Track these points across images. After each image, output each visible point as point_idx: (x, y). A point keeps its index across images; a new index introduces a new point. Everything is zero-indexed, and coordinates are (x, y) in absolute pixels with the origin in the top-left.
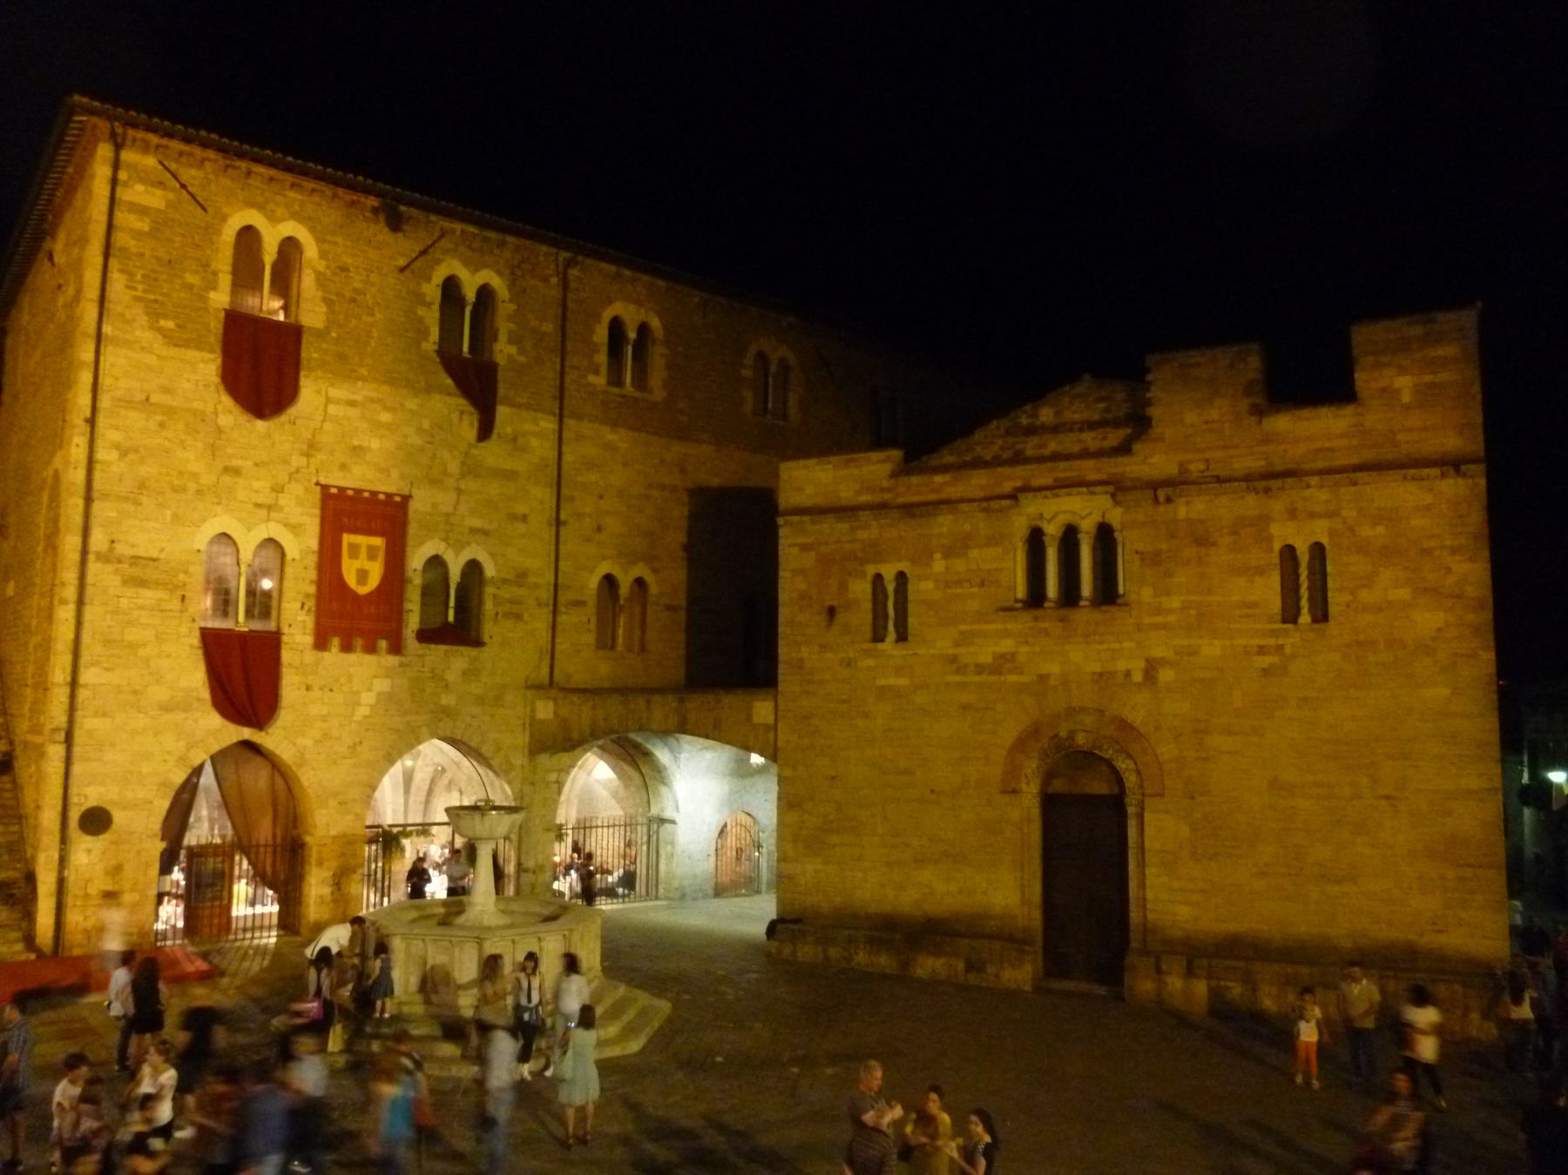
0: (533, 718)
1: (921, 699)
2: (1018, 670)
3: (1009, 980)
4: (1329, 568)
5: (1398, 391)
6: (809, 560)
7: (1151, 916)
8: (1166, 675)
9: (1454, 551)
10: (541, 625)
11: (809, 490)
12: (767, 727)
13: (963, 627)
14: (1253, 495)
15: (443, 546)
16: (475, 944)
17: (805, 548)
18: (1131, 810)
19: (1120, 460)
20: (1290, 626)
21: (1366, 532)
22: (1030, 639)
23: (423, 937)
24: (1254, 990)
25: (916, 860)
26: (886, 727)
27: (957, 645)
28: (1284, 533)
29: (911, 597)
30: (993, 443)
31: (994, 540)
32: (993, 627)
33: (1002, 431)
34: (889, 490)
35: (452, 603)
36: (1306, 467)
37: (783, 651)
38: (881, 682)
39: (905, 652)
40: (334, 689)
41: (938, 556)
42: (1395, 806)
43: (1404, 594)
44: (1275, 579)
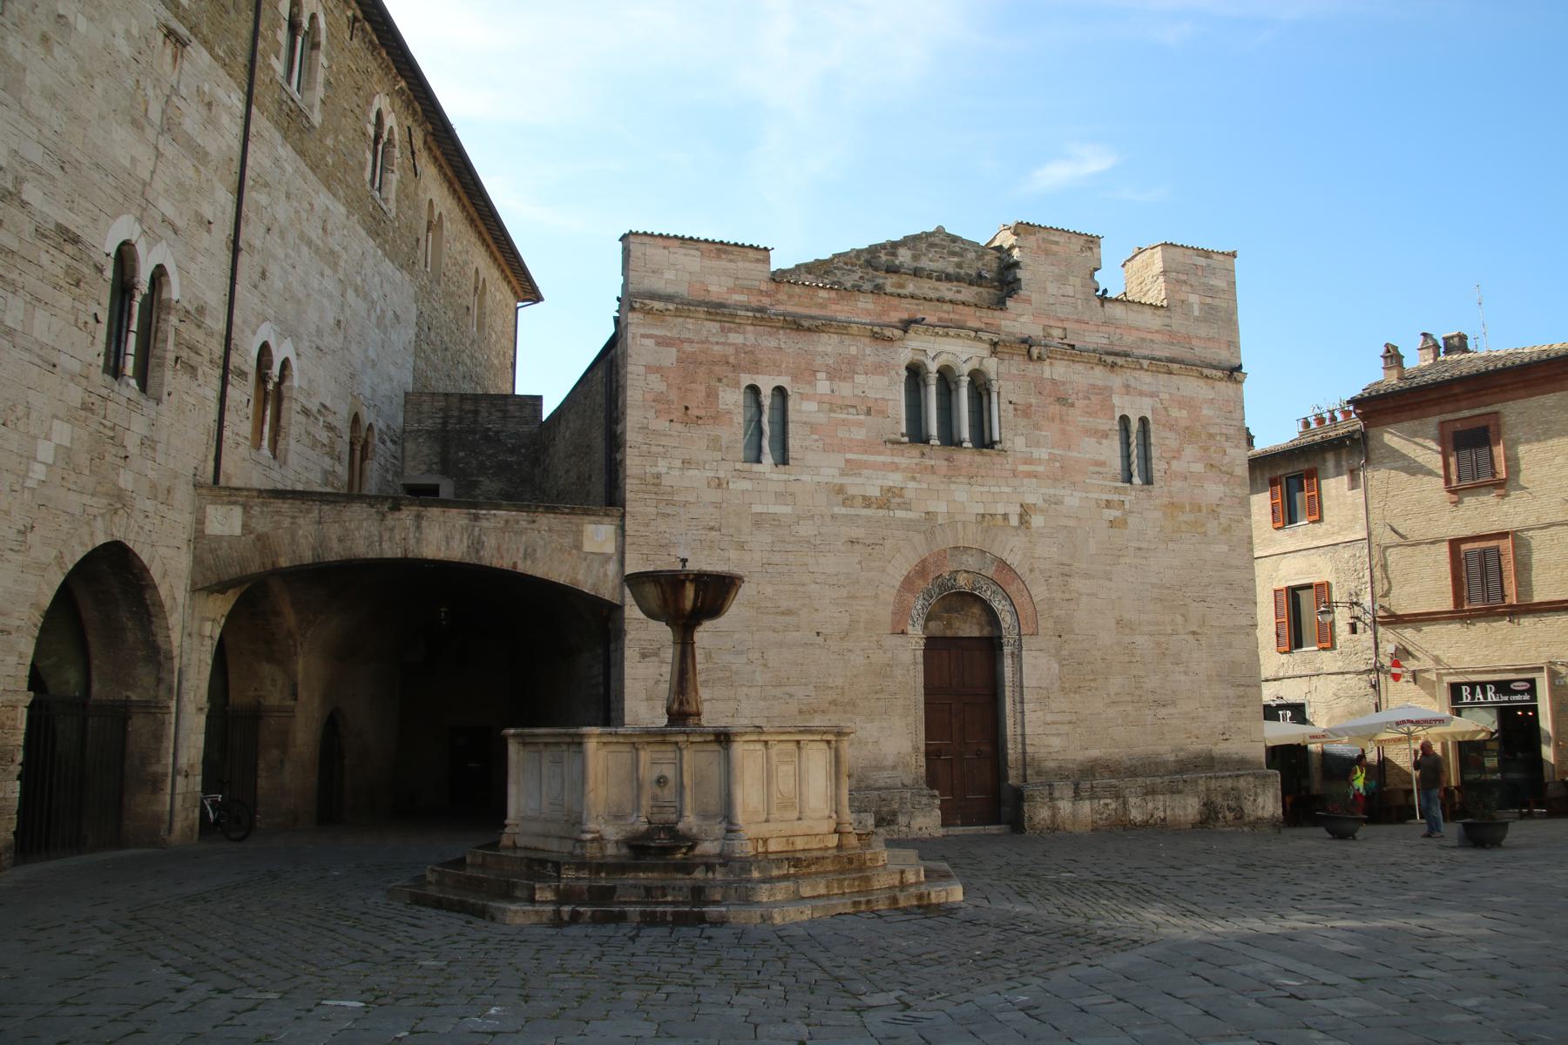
0: (198, 533)
1: (806, 530)
2: (906, 506)
3: (920, 829)
4: (1153, 440)
6: (669, 356)
7: (1029, 750)
8: (1037, 521)
9: (1228, 438)
11: (669, 275)
12: (606, 558)
13: (849, 456)
15: (137, 229)
16: (824, 746)
18: (1007, 650)
19: (997, 313)
20: (1128, 485)
22: (918, 476)
23: (798, 737)
24: (1125, 803)
25: (801, 712)
26: (765, 561)
27: (843, 474)
28: (1124, 405)
29: (792, 416)
30: (854, 272)
31: (879, 369)
35: (134, 327)
36: (1136, 352)
37: (634, 464)
38: (757, 508)
39: (786, 477)
40: (9, 423)
44: (1115, 444)
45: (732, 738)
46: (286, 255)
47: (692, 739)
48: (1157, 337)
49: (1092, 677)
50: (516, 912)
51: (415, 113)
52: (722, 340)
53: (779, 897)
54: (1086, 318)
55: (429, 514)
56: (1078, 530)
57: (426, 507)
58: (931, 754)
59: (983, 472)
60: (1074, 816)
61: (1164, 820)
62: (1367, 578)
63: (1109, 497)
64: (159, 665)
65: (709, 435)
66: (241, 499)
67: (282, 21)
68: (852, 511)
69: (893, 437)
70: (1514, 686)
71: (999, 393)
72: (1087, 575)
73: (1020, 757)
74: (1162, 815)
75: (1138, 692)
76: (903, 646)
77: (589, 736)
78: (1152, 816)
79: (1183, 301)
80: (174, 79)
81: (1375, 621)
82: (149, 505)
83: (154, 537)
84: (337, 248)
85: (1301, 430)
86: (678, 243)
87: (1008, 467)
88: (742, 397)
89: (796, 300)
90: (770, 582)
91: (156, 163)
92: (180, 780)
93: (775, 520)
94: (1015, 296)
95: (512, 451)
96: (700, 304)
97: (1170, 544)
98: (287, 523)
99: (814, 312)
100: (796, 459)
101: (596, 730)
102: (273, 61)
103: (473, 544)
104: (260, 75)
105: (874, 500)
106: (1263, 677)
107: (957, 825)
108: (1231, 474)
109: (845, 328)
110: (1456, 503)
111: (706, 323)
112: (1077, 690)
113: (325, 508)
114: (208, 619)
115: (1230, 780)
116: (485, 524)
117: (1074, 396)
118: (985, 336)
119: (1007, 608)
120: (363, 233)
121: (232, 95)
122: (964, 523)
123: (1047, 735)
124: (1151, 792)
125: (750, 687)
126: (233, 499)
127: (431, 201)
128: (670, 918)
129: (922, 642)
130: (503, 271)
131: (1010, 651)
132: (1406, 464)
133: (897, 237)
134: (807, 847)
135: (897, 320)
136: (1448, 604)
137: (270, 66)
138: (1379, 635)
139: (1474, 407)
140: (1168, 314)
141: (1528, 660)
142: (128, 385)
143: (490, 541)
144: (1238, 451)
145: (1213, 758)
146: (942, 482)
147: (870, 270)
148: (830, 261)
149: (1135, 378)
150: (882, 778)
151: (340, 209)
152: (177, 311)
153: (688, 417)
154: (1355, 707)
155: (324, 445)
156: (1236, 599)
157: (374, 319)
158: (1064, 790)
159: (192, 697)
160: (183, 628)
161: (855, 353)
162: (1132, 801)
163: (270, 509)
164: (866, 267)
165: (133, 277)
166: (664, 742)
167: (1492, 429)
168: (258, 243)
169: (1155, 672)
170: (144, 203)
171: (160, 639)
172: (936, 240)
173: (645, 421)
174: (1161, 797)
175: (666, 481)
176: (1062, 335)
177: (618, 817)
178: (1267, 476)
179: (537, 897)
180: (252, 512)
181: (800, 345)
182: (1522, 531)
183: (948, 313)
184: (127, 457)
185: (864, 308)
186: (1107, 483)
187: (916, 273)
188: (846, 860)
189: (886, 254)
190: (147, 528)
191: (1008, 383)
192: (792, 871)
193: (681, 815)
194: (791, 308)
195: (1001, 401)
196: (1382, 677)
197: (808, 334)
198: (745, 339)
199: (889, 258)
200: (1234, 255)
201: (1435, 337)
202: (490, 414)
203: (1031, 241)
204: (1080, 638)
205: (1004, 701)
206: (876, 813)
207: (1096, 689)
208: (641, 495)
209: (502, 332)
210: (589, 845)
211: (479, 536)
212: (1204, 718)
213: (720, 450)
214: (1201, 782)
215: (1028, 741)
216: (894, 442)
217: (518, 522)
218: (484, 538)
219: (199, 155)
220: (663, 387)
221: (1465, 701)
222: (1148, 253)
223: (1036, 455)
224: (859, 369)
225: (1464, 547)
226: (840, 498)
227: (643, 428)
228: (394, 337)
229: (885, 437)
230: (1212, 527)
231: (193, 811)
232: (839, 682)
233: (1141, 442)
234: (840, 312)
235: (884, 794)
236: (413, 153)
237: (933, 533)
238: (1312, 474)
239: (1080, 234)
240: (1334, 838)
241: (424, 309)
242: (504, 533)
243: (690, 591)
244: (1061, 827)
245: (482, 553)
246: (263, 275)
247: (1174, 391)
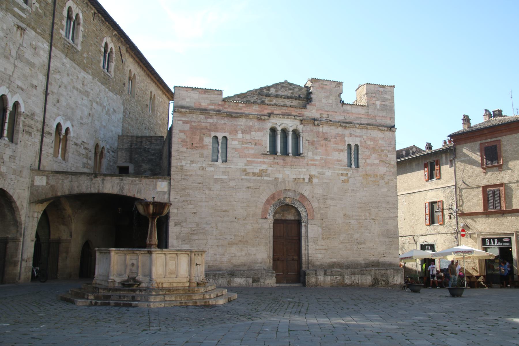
0: (32, 185)
1: (232, 184)
2: (268, 176)
3: (268, 284)
4: (360, 152)
5: (377, 105)
6: (187, 127)
7: (310, 258)
8: (315, 180)
9: (389, 151)
10: (37, 140)
11: (188, 100)
12: (164, 193)
13: (248, 159)
14: (341, 127)
15: (7, 90)
16: (187, 255)
17: (185, 122)
18: (303, 224)
19: (303, 110)
20: (350, 168)
21: (369, 143)
22: (272, 165)
24: (343, 277)
25: (229, 244)
26: (218, 194)
27: (246, 165)
28: (349, 140)
29: (229, 146)
30: (254, 96)
31: (260, 130)
32: (259, 160)
33: (257, 93)
34: (221, 105)
35: (7, 121)
36: (355, 122)
37: (174, 162)
38: (215, 177)
39: (226, 166)
41: (239, 132)
42: (374, 222)
43: (377, 162)
45: (152, 252)
46: (67, 94)
47: (141, 252)
48: (363, 116)
49: (334, 234)
50: (80, 302)
51: (122, 42)
52: (205, 121)
53: (157, 300)
54: (336, 111)
55: (106, 179)
56: (330, 184)
57: (105, 176)
58: (274, 259)
59: (296, 164)
60: (324, 281)
61: (358, 283)
62: (455, 200)
63: (343, 172)
64: (17, 226)
65: (200, 153)
66: (46, 174)
67: (64, 18)
68: (248, 178)
69: (264, 152)
70: (504, 240)
71: (303, 137)
72: (333, 199)
73: (307, 260)
74: (357, 282)
75: (351, 239)
76: (265, 222)
77: (112, 251)
78: (353, 282)
79: (373, 104)
80: (21, 42)
81: (457, 215)
82: (13, 177)
83: (15, 186)
84: (89, 90)
85: (443, 145)
86: (191, 89)
87: (305, 162)
88: (211, 140)
89: (231, 107)
90: (219, 201)
91: (14, 69)
92: (24, 263)
93: (222, 181)
94: (310, 104)
95: (153, 155)
96: (198, 109)
97: (365, 188)
98: (60, 181)
99: (238, 111)
100: (230, 160)
101: (114, 249)
102: (61, 31)
103: (121, 188)
104: (55, 36)
105: (256, 174)
106: (400, 235)
107: (284, 283)
108: (390, 164)
109: (248, 116)
110: (485, 173)
111: (200, 116)
112: (328, 238)
113: (73, 177)
114: (36, 212)
115: (384, 271)
116: (125, 182)
117: (331, 137)
118: (298, 118)
119: (304, 210)
120: (100, 84)
121: (44, 44)
122: (288, 181)
123: (317, 253)
124: (353, 274)
125: (211, 235)
126: (43, 174)
127: (130, 70)
128: (122, 305)
129: (272, 221)
130: (163, 91)
132: (469, 158)
133: (270, 84)
134: (177, 286)
135: (267, 113)
136: (481, 209)
137: (59, 33)
138: (458, 220)
139: (492, 138)
140: (367, 108)
141: (509, 230)
142: (4, 139)
143: (126, 187)
144: (392, 156)
145: (379, 263)
146: (281, 168)
147: (260, 96)
148: (246, 93)
149: (354, 131)
150: (257, 266)
151: (91, 77)
152: (23, 115)
153: (193, 147)
154: (450, 246)
155: (84, 155)
156: (390, 207)
157: (104, 111)
158: (321, 273)
159: (29, 237)
160: (26, 215)
161: (251, 124)
162: (346, 277)
163: (55, 177)
164: (259, 95)
165: (6, 106)
166: (133, 253)
167: (498, 146)
168: (56, 91)
169: (358, 232)
170: (10, 82)
171: (18, 219)
172: (284, 85)
173: (178, 148)
174: (357, 276)
175: (185, 168)
176: (327, 117)
177: (120, 275)
178: (423, 162)
179: (89, 298)
180: (50, 178)
181: (232, 122)
182: (508, 184)
183: (285, 110)
184: (4, 162)
185: (255, 109)
186: (342, 167)
187: (277, 96)
188: (187, 290)
189: (266, 90)
190: (12, 184)
191: (307, 134)
192: (167, 293)
193: (137, 275)
194: (229, 110)
195: (304, 140)
196: (459, 235)
197: (235, 118)
198: (213, 121)
199: (267, 91)
200: (394, 86)
201: (490, 111)
202: (146, 142)
203: (317, 85)
204: (330, 220)
205: (302, 242)
206: (252, 278)
207: (335, 238)
208: (176, 172)
209: (163, 112)
210: (110, 283)
211: (123, 186)
212: (376, 249)
213: (204, 157)
214: (373, 271)
215: (309, 255)
216: (264, 154)
217: (135, 181)
218: (125, 187)
219: (32, 65)
220: (185, 137)
221: (487, 245)
222: (362, 86)
223: (316, 158)
224: (253, 130)
225: (488, 189)
226: (245, 173)
227: (178, 151)
228: (113, 117)
229: (261, 153)
230: (382, 182)
231: (29, 273)
232: (242, 234)
233: (356, 153)
234: (246, 111)
235: (255, 272)
236: (121, 55)
237: (277, 185)
238: (438, 163)
239: (335, 81)
240: (412, 292)
241: (127, 107)
242: (131, 185)
243: (151, 207)
244: (319, 285)
245: (123, 191)
246: (58, 101)
247: (369, 135)
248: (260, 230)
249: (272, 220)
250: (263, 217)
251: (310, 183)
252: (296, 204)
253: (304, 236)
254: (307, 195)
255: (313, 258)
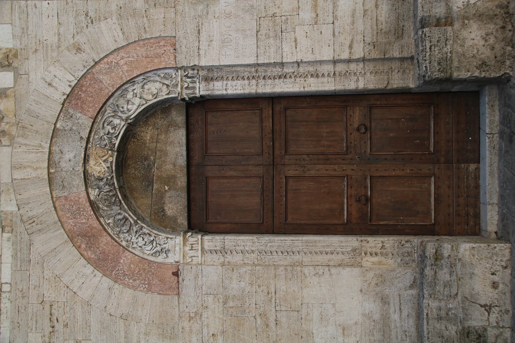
3: (495, 285)
7: (359, 53)
73: (370, 66)
76: (196, 277)
107: (478, 169)
119: (137, 88)
122: (13, 168)
123: (335, 17)
131: (203, 84)
215: (345, 56)
237: (32, 220)
248: (231, 304)
249: (185, 240)
250: (174, 285)
251: (15, 64)
252: (114, 128)
253: (254, 82)
254: (73, 79)
255: (360, 37)
